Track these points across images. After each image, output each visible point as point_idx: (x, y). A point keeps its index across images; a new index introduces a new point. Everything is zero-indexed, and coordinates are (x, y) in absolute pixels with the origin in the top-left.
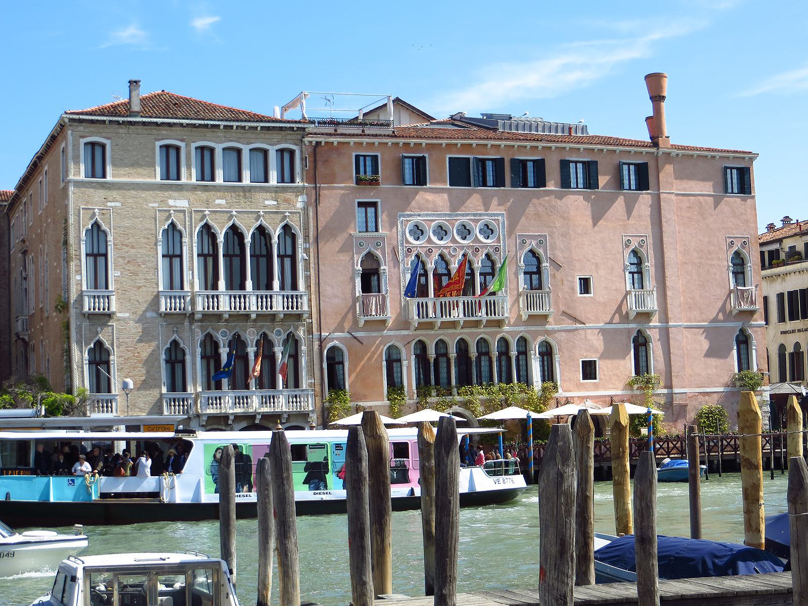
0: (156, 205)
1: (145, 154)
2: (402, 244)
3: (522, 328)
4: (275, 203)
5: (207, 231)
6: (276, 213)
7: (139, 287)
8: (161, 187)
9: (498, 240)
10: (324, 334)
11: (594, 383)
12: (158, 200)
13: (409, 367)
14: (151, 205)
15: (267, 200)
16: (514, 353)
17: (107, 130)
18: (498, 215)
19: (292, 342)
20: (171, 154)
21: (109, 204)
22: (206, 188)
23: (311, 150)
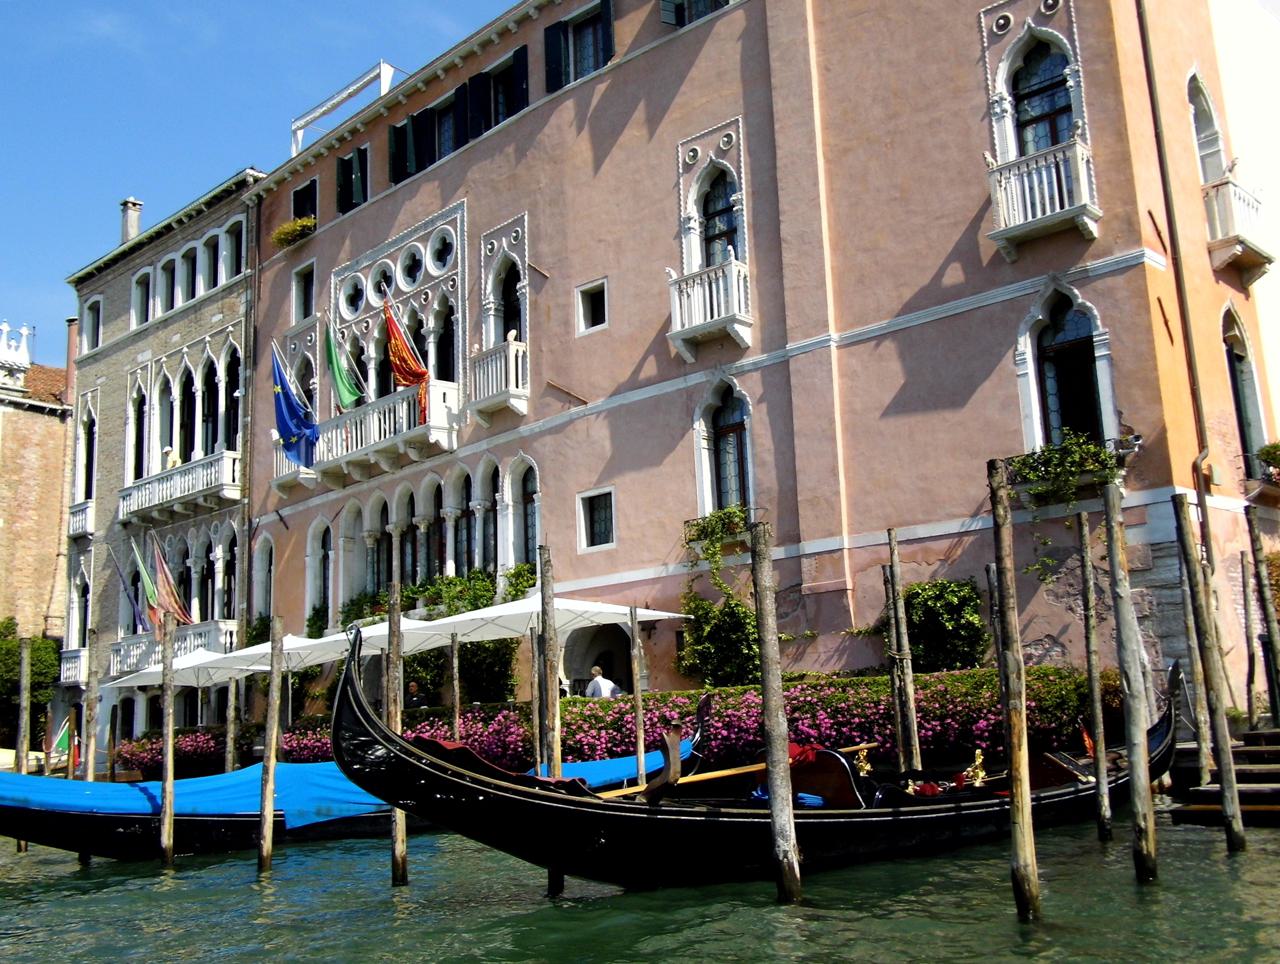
3: (484, 445)
9: (455, 266)
11: (608, 553)
13: (336, 562)
21: (99, 382)
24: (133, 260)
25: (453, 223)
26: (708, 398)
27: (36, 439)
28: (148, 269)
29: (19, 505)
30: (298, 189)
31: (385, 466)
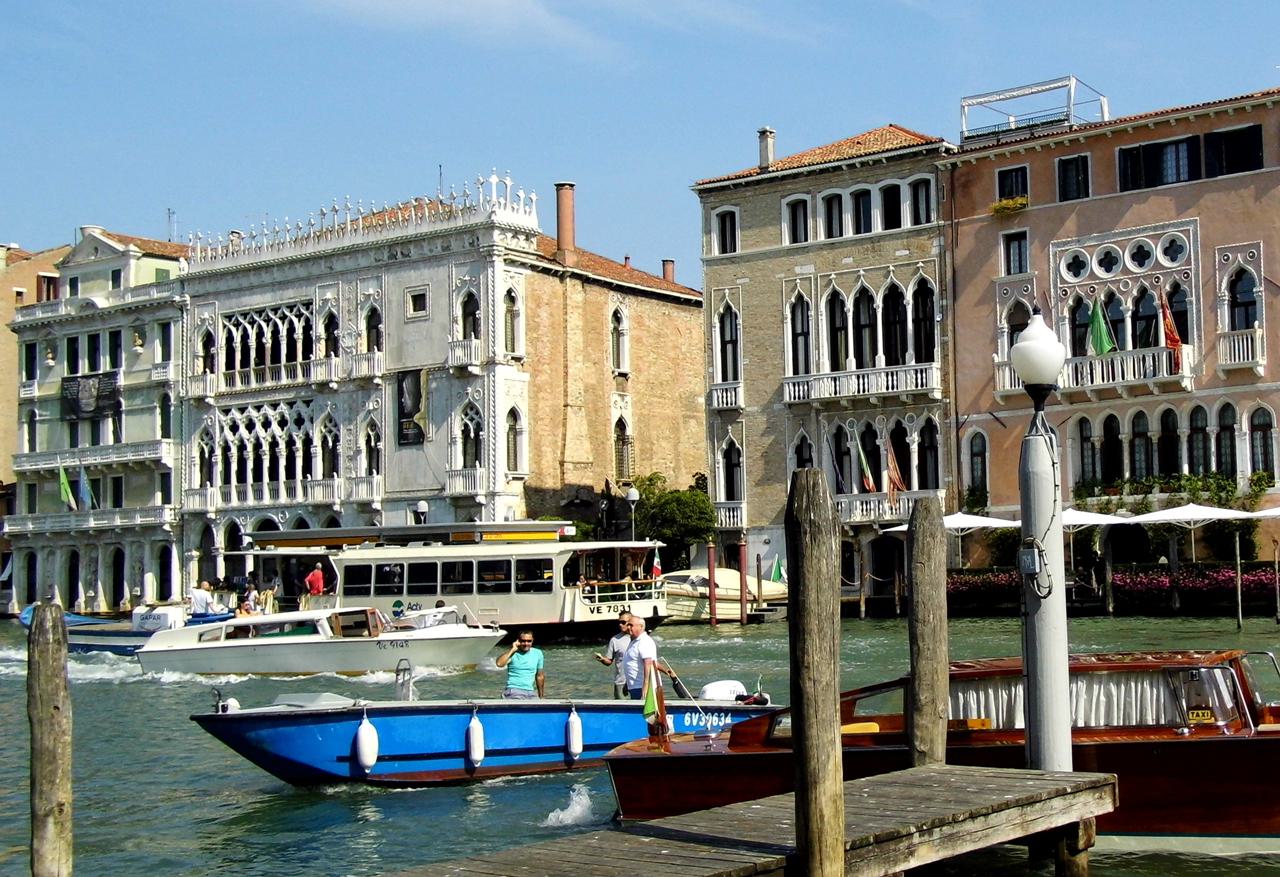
0: (783, 275)
1: (771, 216)
2: (1055, 286)
3: (1221, 391)
4: (907, 252)
5: (835, 301)
6: (908, 265)
7: (767, 375)
8: (789, 252)
9: (1188, 262)
12: (785, 268)
14: (779, 276)
16: (1212, 428)
17: (735, 196)
18: (1187, 223)
19: (928, 430)
20: (798, 209)
21: (738, 281)
22: (732, 261)
23: (948, 175)
27: (545, 298)
28: (807, 197)
29: (538, 360)
31: (1125, 396)
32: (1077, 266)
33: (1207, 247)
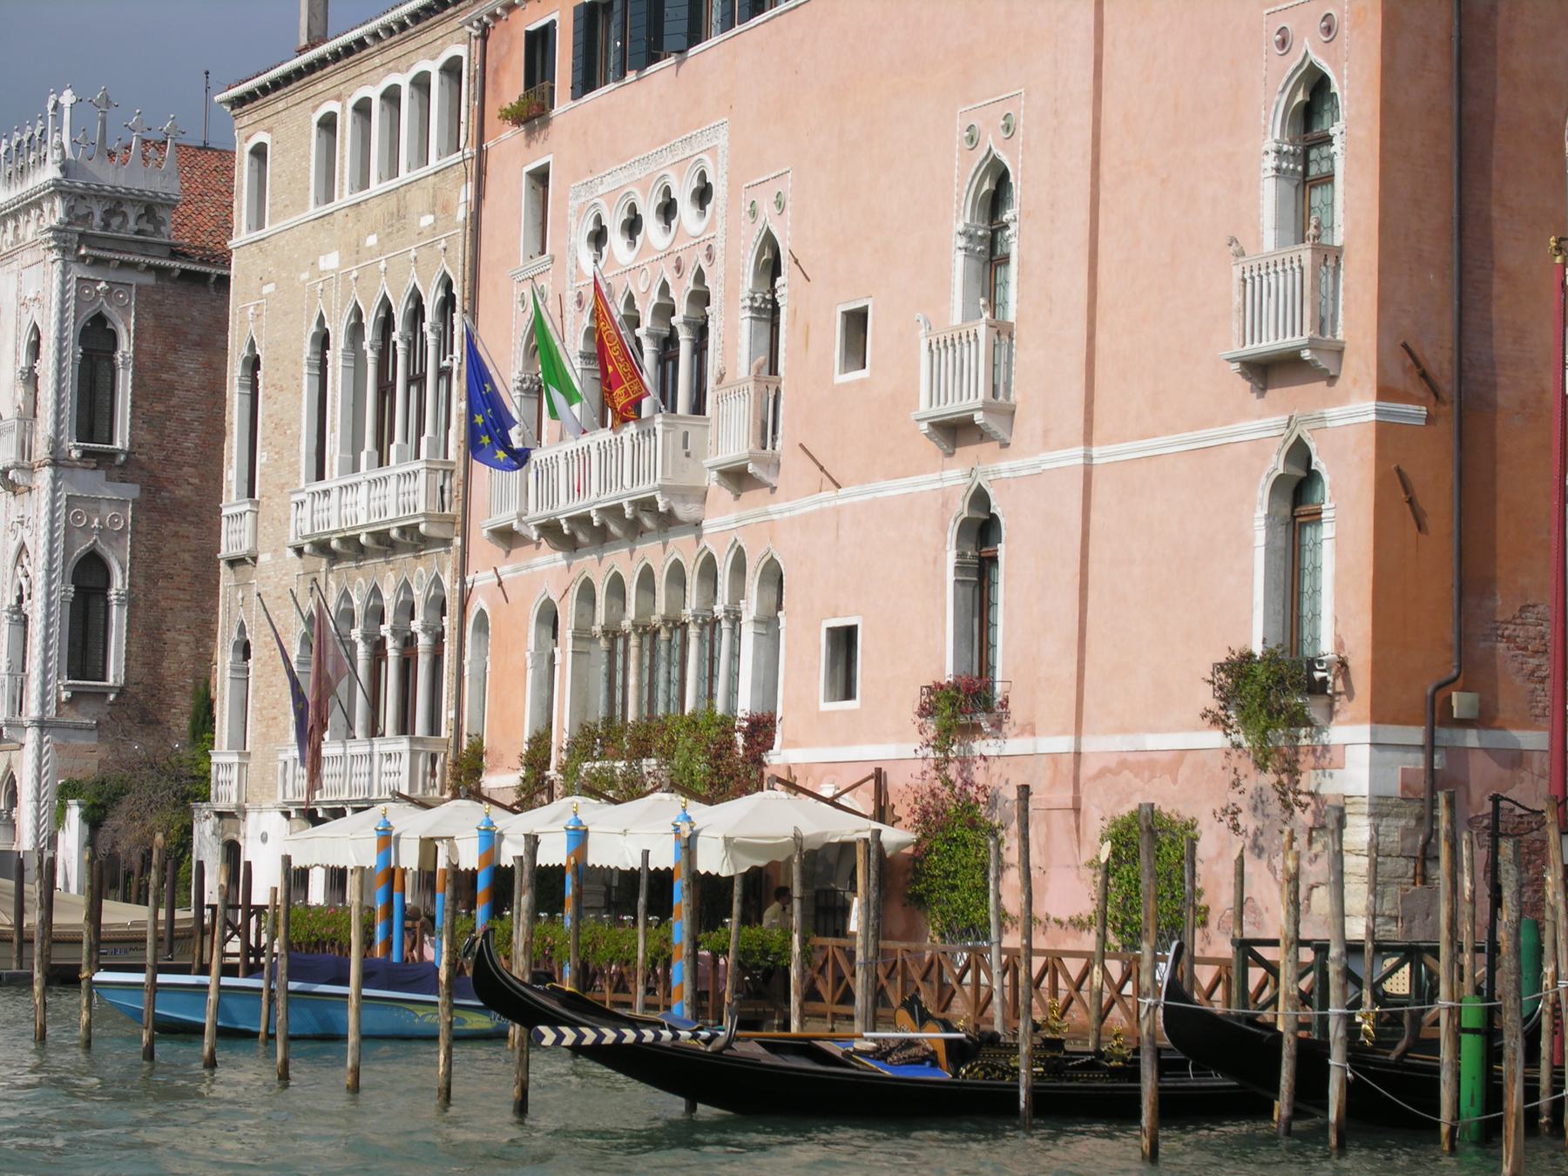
10: (469, 579)
11: (850, 712)
15: (423, 214)
24: (313, 83)
25: (711, 150)
26: (961, 508)
29: (166, 458)
30: (531, 28)
32: (598, 237)
33: (732, 185)
